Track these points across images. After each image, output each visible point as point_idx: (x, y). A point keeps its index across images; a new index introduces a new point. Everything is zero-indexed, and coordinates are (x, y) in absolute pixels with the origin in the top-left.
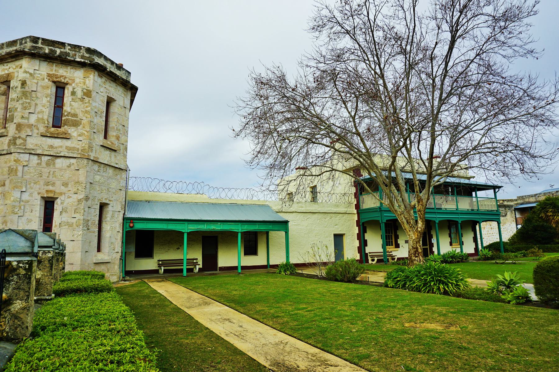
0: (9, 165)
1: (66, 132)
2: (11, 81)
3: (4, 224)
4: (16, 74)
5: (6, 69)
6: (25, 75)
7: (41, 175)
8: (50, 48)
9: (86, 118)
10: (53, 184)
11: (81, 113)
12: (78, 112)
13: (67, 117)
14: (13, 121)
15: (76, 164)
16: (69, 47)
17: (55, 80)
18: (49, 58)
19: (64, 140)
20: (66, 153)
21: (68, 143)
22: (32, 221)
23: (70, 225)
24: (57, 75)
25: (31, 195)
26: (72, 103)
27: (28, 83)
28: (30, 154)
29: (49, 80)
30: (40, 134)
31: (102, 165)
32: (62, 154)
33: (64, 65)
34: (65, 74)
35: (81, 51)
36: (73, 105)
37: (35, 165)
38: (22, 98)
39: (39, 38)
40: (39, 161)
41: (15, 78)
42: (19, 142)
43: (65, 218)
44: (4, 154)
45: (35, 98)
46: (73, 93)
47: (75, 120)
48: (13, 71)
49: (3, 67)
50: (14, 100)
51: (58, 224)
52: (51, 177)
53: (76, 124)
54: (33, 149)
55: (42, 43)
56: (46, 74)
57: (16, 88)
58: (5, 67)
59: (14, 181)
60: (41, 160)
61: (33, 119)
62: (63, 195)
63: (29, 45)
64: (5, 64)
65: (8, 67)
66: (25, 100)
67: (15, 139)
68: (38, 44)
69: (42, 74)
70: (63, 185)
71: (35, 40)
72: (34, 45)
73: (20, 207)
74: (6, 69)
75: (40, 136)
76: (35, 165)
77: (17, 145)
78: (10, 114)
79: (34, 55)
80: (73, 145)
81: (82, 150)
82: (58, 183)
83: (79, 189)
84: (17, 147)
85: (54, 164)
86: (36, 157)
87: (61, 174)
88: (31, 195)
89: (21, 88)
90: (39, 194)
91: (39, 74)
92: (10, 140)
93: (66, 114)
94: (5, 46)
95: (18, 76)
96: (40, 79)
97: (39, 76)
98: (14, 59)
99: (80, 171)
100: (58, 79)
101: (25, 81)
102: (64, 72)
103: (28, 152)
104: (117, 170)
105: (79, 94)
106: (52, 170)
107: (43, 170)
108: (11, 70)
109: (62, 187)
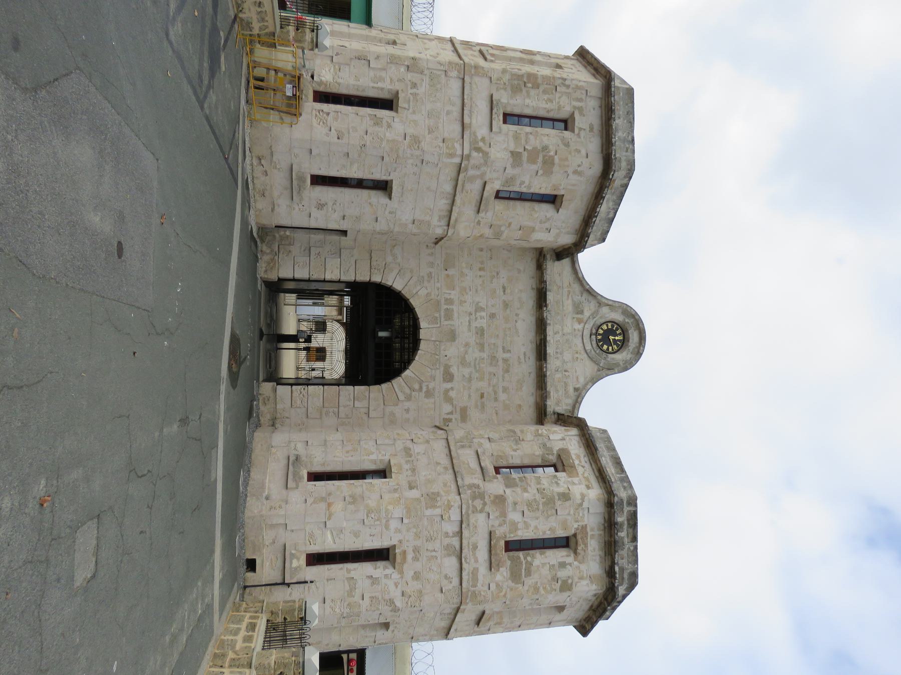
0: (442, 493)
1: (500, 564)
3: (351, 500)
4: (576, 480)
5: (580, 462)
6: (578, 497)
7: (430, 539)
8: (626, 522)
9: (527, 591)
10: (416, 559)
11: (533, 581)
13: (524, 562)
14: (507, 486)
15: (450, 587)
16: (632, 548)
17: (579, 537)
18: (610, 526)
19: (487, 564)
20: (467, 571)
21: (483, 570)
22: (357, 538)
23: (351, 593)
24: (587, 539)
25: (398, 531)
26: (548, 566)
27: (568, 503)
28: (462, 522)
29: (577, 529)
30: (493, 529)
31: (452, 617)
32: (465, 565)
33: (603, 545)
34: (590, 548)
35: (630, 565)
37: (444, 530)
38: (544, 498)
39: (636, 506)
41: (570, 479)
42: (478, 503)
43: (363, 585)
44: (457, 481)
45: (546, 515)
46: (563, 565)
48: (580, 475)
49: (582, 456)
50: (539, 483)
51: (353, 574)
52: (429, 554)
53: (515, 576)
54: (468, 525)
55: (630, 511)
56: (584, 524)
57: (557, 484)
58: (582, 459)
59: (419, 507)
60: (453, 537)
61: (514, 516)
62: (400, 576)
63: (622, 494)
64: (586, 459)
65: (583, 463)
67: (481, 496)
68: (627, 506)
71: (633, 501)
72: (625, 502)
73: (378, 520)
74: (580, 462)
75: (490, 529)
77: (472, 502)
78: (517, 480)
79: (610, 504)
80: (480, 577)
81: (474, 592)
82: (418, 566)
83: (411, 598)
84: (470, 502)
85: (449, 555)
86: (457, 529)
87: (433, 568)
88: (398, 531)
89: (559, 494)
90: (400, 541)
91: (584, 515)
92: (479, 485)
93: (529, 559)
94: (612, 453)
95: (574, 484)
96: (576, 517)
97: (581, 515)
98: (597, 474)
99: (440, 595)
100: (580, 540)
101: (570, 499)
102: (593, 547)
103: (464, 519)
104: (446, 631)
105: (562, 574)
106: (438, 554)
107: (438, 541)
108: (580, 470)
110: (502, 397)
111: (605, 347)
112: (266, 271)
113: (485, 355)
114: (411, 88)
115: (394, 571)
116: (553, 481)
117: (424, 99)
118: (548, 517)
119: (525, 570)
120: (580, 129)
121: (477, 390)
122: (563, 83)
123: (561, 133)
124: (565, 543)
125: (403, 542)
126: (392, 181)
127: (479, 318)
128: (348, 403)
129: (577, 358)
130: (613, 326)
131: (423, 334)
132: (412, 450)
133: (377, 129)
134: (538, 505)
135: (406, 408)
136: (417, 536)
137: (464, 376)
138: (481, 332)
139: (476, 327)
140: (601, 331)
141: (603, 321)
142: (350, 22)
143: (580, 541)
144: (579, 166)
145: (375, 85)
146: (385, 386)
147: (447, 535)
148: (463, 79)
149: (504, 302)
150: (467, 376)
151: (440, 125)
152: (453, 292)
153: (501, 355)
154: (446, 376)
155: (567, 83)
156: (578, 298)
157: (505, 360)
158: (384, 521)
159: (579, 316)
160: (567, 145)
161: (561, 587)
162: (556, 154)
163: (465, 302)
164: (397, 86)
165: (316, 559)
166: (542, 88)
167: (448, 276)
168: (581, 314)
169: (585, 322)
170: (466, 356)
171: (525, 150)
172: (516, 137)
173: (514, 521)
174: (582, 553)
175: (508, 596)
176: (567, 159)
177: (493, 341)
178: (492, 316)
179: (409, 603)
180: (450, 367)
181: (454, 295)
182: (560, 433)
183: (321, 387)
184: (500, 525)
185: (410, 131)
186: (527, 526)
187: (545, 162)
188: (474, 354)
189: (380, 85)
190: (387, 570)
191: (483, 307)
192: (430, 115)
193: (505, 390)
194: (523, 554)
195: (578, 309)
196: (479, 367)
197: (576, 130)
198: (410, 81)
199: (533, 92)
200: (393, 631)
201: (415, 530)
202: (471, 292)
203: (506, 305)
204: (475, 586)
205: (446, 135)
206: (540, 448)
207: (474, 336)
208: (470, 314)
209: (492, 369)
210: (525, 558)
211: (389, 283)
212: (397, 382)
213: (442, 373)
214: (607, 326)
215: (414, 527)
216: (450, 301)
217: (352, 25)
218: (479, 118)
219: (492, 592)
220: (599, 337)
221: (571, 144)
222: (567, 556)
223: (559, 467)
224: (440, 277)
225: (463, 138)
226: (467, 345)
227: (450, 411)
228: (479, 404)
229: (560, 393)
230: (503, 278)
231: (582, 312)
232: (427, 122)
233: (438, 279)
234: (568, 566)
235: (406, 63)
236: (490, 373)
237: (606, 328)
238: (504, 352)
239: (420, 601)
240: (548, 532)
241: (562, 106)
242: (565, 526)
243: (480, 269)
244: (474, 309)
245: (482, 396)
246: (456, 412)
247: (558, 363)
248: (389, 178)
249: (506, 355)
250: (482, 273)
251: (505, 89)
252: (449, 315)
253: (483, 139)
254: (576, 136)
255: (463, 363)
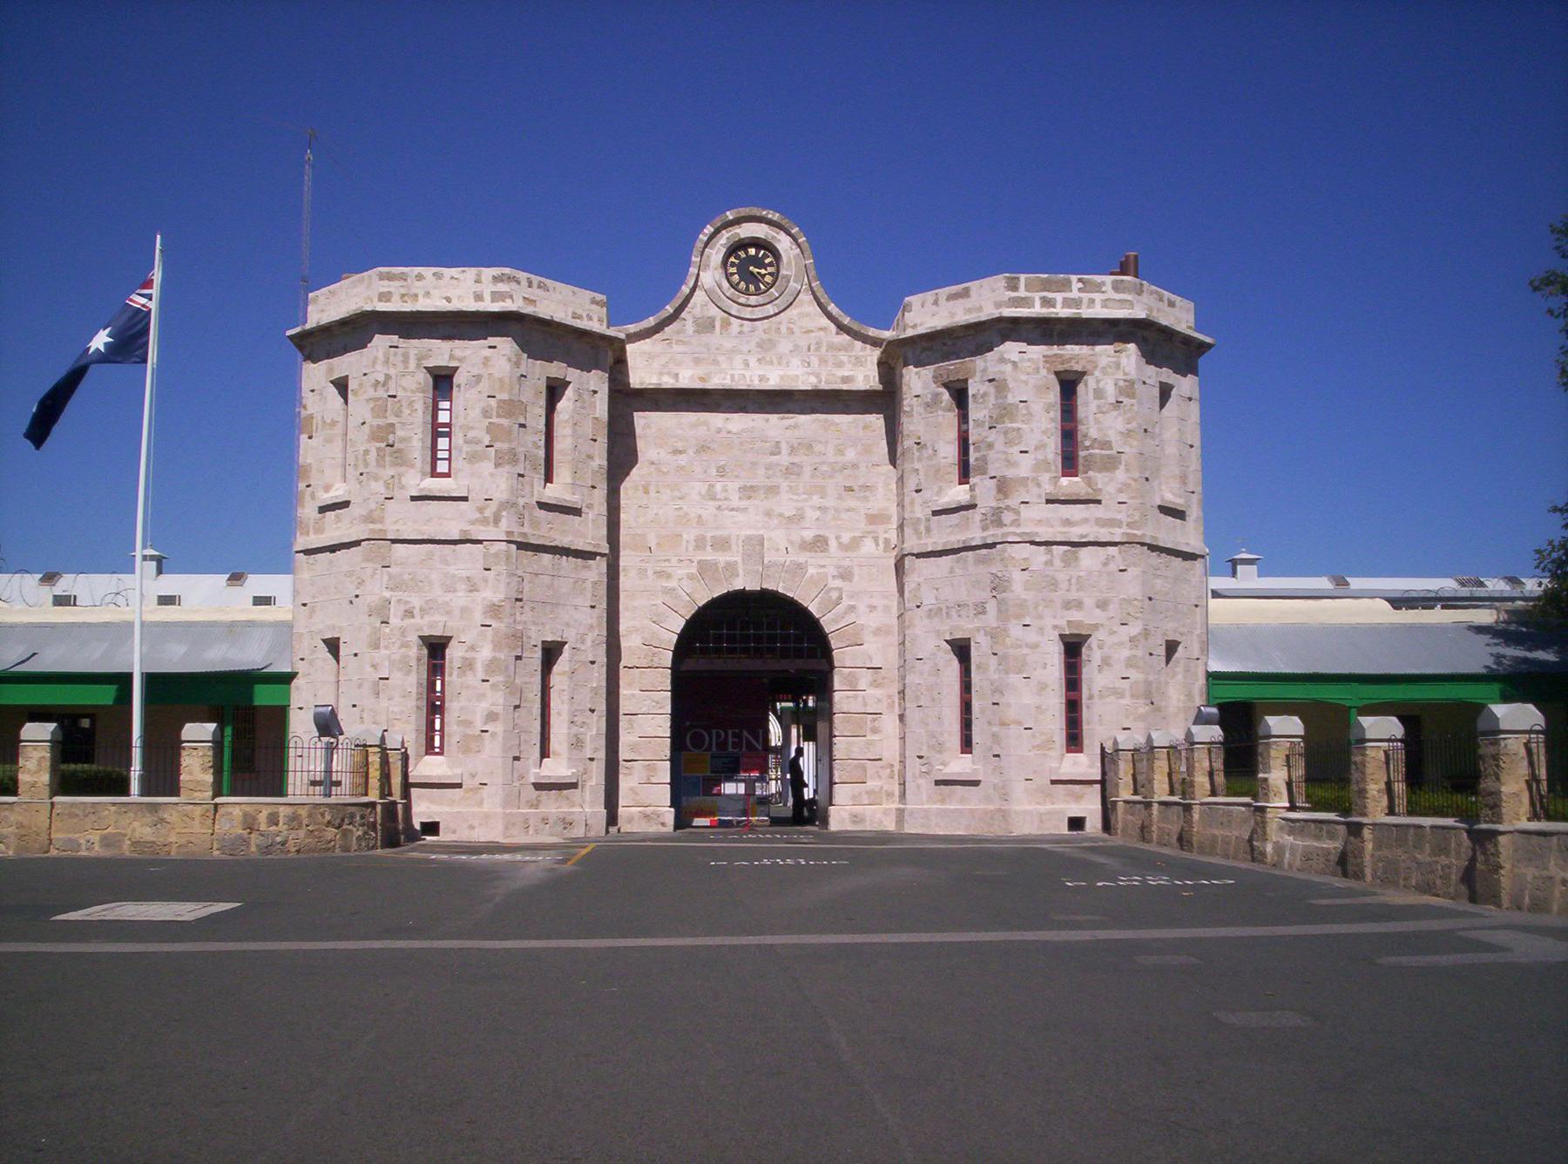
2: (970, 381)
9: (1131, 447)
10: (1079, 605)
12: (1112, 436)
15: (1119, 558)
17: (1060, 368)
25: (1041, 630)
29: (1048, 370)
32: (1091, 539)
36: (1101, 420)
37: (1042, 567)
40: (1049, 556)
42: (1007, 517)
45: (1027, 417)
46: (1099, 393)
47: (1109, 456)
52: (1074, 588)
53: (1110, 464)
56: (1042, 359)
57: (985, 395)
60: (1052, 555)
62: (1101, 629)
66: (1009, 425)
69: (1033, 359)
70: (1098, 607)
76: (1041, 567)
77: (1005, 525)
80: (1109, 515)
82: (1089, 602)
84: (1005, 530)
85: (1077, 559)
89: (996, 398)
91: (1029, 360)
95: (985, 370)
100: (1065, 366)
109: (1097, 610)
110: (851, 455)
111: (768, 279)
112: (663, 824)
113: (784, 485)
114: (413, 617)
115: (1093, 636)
116: (981, 400)
117: (428, 598)
118: (1031, 414)
119: (1102, 449)
120: (452, 357)
121: (840, 498)
122: (384, 385)
123: (459, 386)
124: (1069, 384)
125: (1056, 624)
126: (543, 642)
127: (724, 494)
128: (860, 699)
129: (788, 328)
130: (733, 265)
131: (753, 585)
132: (930, 607)
133: (479, 667)
134: (1014, 429)
135: (868, 610)
136: (1049, 603)
137: (817, 519)
138: (748, 491)
139: (740, 498)
140: (743, 285)
141: (726, 284)
142: (289, 706)
143: (1066, 367)
144: (509, 360)
145: (415, 667)
146: (834, 643)
147: (1049, 563)
148: (394, 541)
149: (697, 452)
150: (818, 513)
151: (465, 574)
152: (684, 536)
153: (784, 459)
154: (818, 547)
155: (381, 378)
156: (690, 327)
157: (793, 450)
158: (1026, 651)
159: (718, 324)
160: (478, 378)
161: (1128, 396)
162: (494, 397)
163: (700, 516)
164: (413, 638)
165: (1074, 740)
166: (392, 419)
167: (658, 544)
168: (714, 321)
169: (726, 315)
170: (787, 514)
171: (492, 446)
172: (473, 458)
173: (1035, 464)
174: (1082, 363)
175: (1137, 475)
176: (501, 380)
177: (761, 471)
178: (722, 472)
179: (1137, 615)
180: (803, 542)
181: (689, 535)
182: (910, 377)
183: (835, 740)
184: (1039, 485)
185: (479, 618)
186: (1041, 446)
187: (509, 415)
188: (786, 504)
189: (413, 663)
190: (1092, 646)
191: (706, 487)
192: (450, 589)
193: (840, 452)
194: (1082, 450)
195: (706, 326)
196: (804, 493)
197: (453, 364)
198: (402, 620)
199: (400, 433)
200: (1181, 634)
201: (1041, 608)
202: (685, 508)
203: (703, 448)
204: (1119, 524)
205: (480, 565)
206: (931, 413)
207: (756, 502)
208: (719, 508)
209: (807, 470)
210: (1087, 448)
211: (675, 637)
212: (828, 624)
213: (813, 554)
214: (733, 274)
215: (1036, 608)
216: (700, 543)
217: (294, 704)
218: (449, 520)
219: (1130, 498)
220: (752, 288)
221: (475, 371)
222: (1086, 385)
223: (959, 386)
224: (661, 558)
225: (480, 542)
226: (768, 514)
227: (873, 540)
228: (862, 494)
229: (845, 359)
230: (658, 453)
231: (712, 321)
232: (461, 594)
233: (665, 561)
234: (1101, 385)
235: (378, 625)
236: (812, 476)
237: (742, 283)
238: (779, 453)
239: (1136, 599)
240: (1052, 414)
241: (415, 385)
242: (1042, 389)
243: (646, 492)
244: (712, 503)
245: (850, 489)
246: (874, 532)
247: (796, 362)
248: (540, 646)
249: (784, 448)
250: (652, 489)
251: (400, 475)
252: (722, 544)
253: (481, 510)
254: (464, 365)
255: (797, 518)
